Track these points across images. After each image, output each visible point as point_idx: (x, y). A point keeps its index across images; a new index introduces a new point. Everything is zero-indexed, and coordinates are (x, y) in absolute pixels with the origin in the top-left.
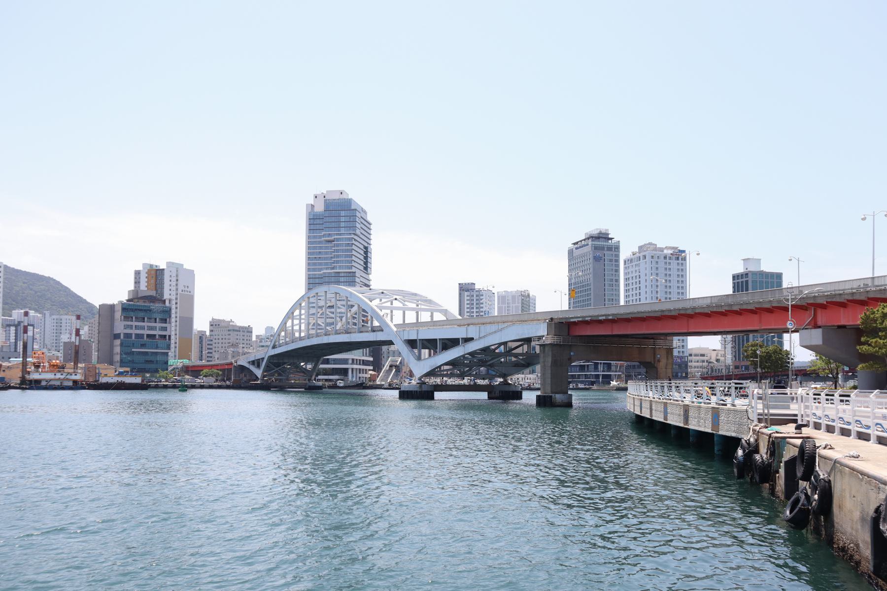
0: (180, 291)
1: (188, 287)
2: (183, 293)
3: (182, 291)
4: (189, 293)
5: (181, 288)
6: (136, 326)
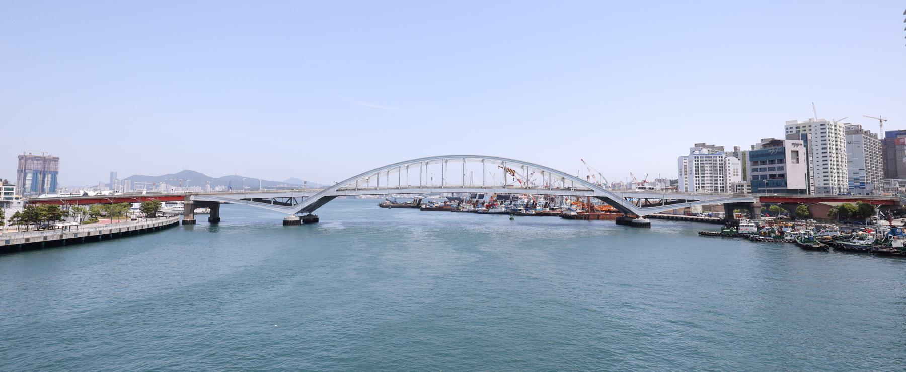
6: (760, 168)
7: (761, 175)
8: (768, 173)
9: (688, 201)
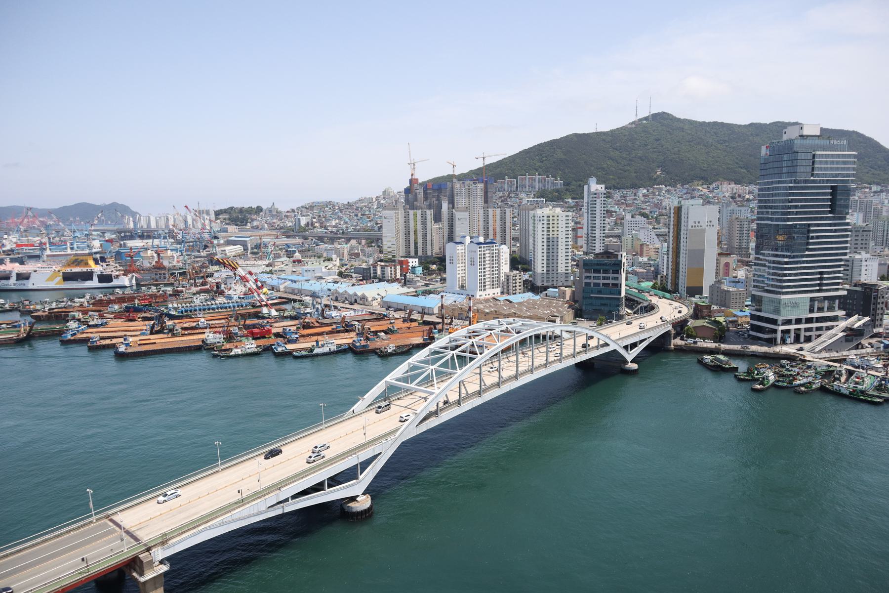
0: (690, 227)
1: (699, 222)
2: (693, 228)
3: (692, 227)
4: (700, 228)
5: (691, 223)
6: (594, 277)
7: (594, 283)
8: (602, 281)
9: (649, 338)
